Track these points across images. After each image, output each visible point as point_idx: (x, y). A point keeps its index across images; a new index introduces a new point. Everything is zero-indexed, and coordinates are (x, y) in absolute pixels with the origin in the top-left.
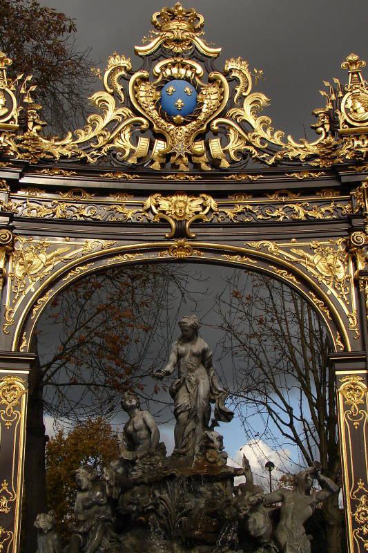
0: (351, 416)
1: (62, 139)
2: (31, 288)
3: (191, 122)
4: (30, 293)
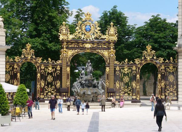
1: (73, 34)
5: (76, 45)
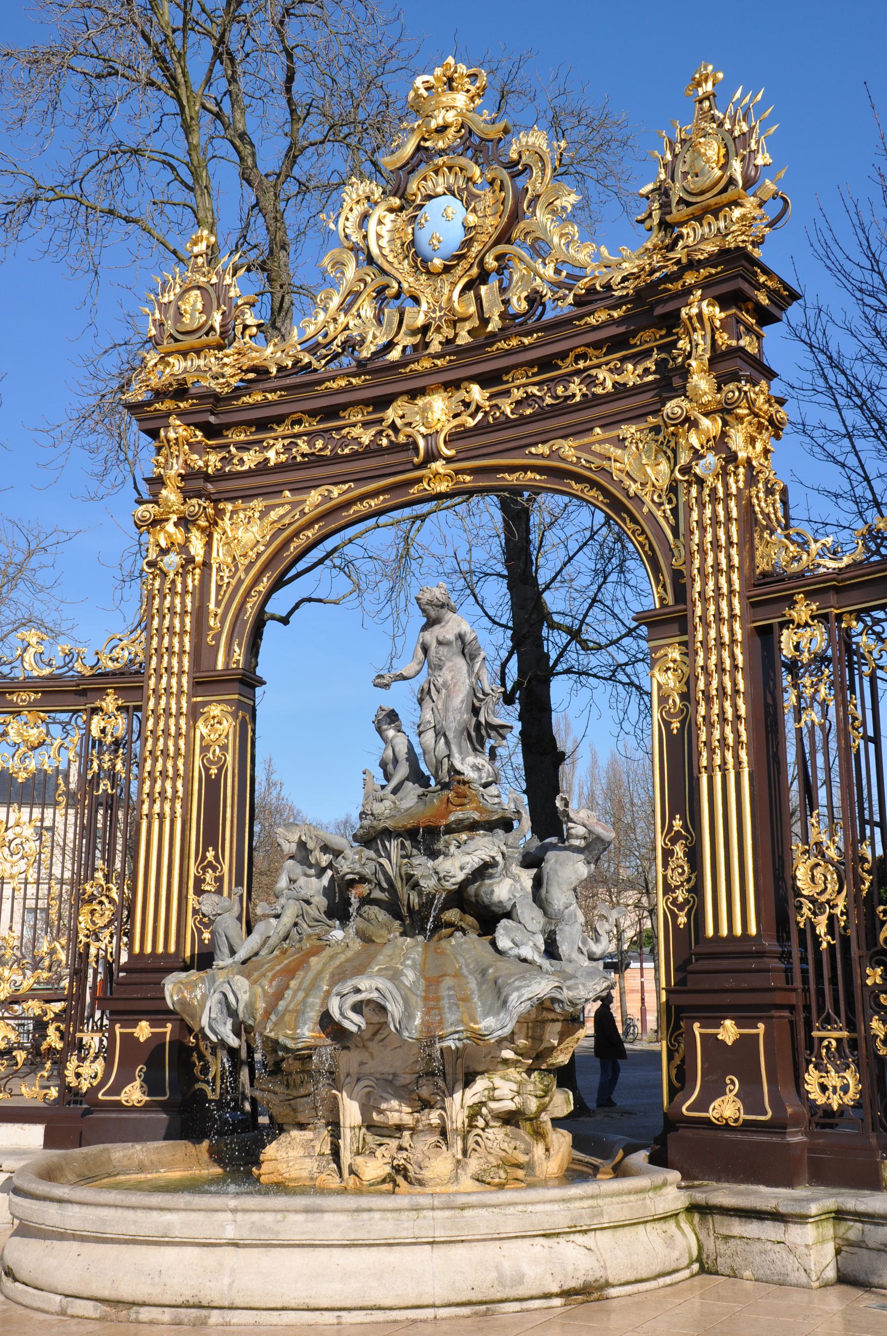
0: (668, 712)
2: (241, 574)
3: (458, 264)
4: (240, 582)
5: (312, 436)
